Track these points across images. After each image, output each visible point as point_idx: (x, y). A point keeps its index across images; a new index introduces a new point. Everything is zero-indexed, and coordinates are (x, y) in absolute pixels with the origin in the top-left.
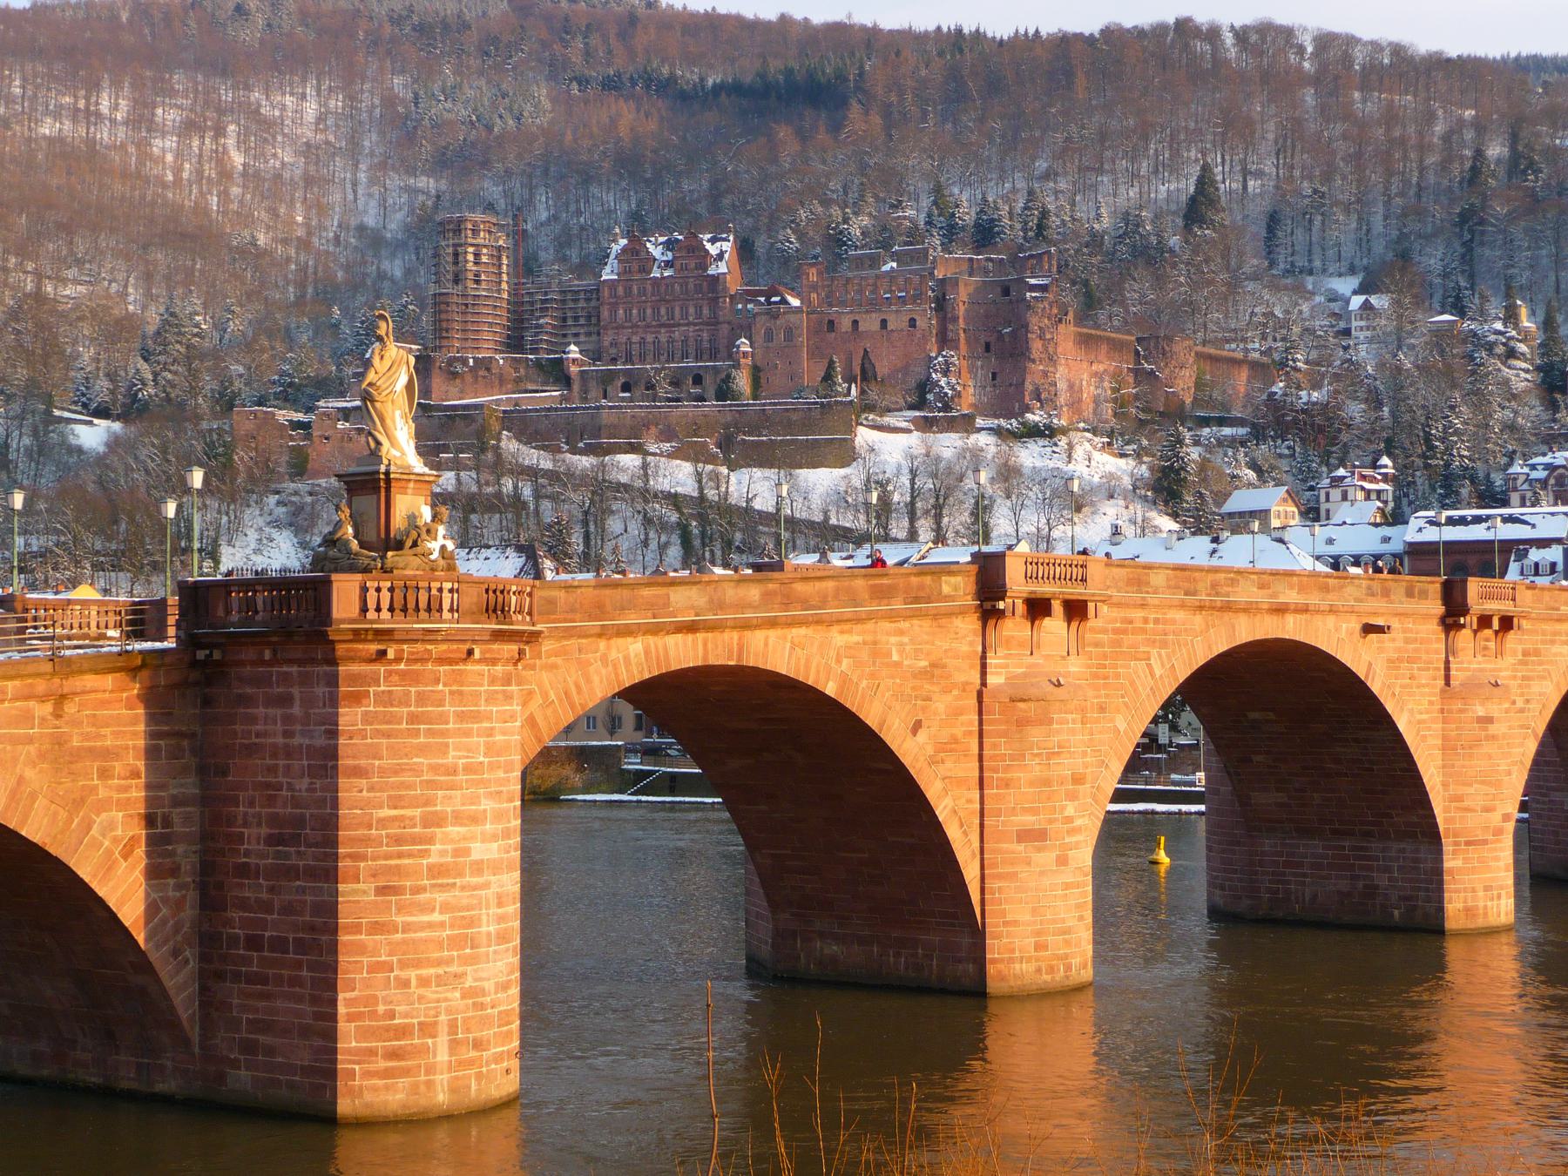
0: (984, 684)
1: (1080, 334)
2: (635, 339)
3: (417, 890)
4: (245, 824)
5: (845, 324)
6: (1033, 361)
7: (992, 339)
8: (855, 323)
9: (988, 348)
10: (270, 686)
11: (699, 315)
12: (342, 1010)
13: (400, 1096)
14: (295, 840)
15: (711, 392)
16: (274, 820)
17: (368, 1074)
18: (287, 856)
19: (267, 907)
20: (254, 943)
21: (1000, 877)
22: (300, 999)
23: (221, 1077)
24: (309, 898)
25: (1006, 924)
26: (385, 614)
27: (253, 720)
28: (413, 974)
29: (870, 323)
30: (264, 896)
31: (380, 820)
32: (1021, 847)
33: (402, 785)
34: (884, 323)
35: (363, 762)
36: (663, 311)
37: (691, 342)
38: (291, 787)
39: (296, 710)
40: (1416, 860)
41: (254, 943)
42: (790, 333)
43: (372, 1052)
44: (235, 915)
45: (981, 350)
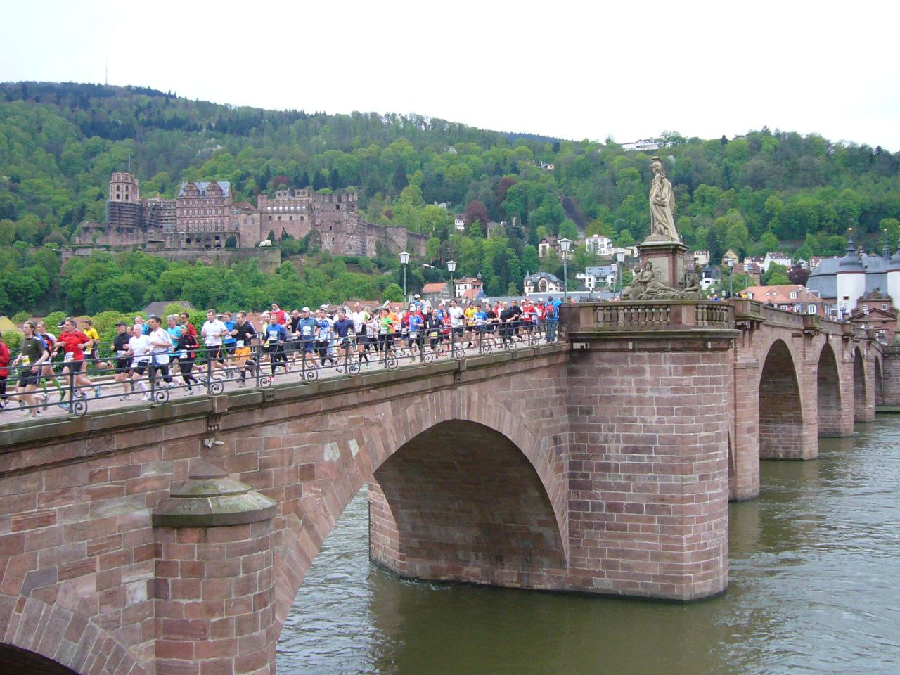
0: (736, 360)
3: (714, 476)
4: (606, 441)
5: (276, 217)
8: (280, 217)
10: (626, 362)
11: (216, 213)
12: (685, 544)
13: (709, 589)
14: (648, 450)
15: (223, 244)
16: (628, 439)
17: (698, 579)
18: (640, 459)
19: (626, 488)
20: (614, 507)
21: (743, 449)
22: (653, 538)
23: (589, 582)
24: (658, 483)
25: (744, 471)
26: (706, 324)
27: (613, 383)
28: (713, 522)
29: (286, 218)
30: (623, 481)
31: (701, 438)
32: (748, 435)
33: (710, 419)
34: (291, 217)
35: (693, 406)
38: (643, 420)
39: (647, 377)
40: (791, 432)
41: (614, 507)
42: (253, 221)
43: (698, 566)
44: (599, 492)
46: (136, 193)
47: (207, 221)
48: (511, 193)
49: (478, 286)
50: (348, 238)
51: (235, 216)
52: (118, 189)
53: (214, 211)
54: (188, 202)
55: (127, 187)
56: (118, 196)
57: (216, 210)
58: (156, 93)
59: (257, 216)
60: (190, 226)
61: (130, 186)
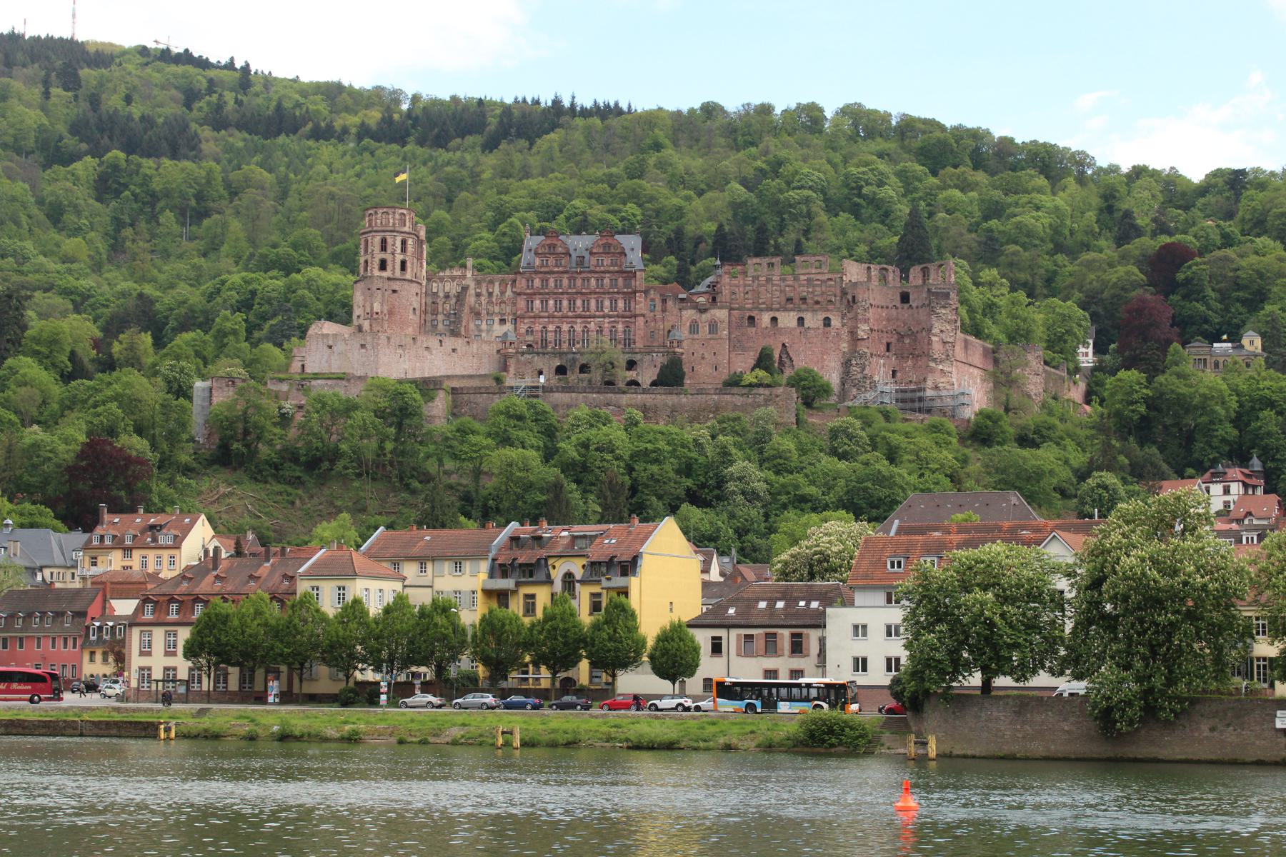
2: (551, 327)
5: (765, 319)
7: (893, 340)
8: (774, 320)
9: (888, 345)
11: (614, 307)
34: (801, 320)
36: (579, 303)
37: (606, 332)
42: (713, 327)
45: (883, 348)
46: (420, 259)
47: (592, 326)
48: (1188, 281)
49: (1254, 487)
50: (932, 371)
51: (659, 316)
52: (384, 247)
53: (607, 303)
54: (545, 282)
55: (404, 243)
56: (383, 265)
57: (614, 302)
58: (203, 63)
59: (721, 314)
60: (551, 337)
61: (410, 242)
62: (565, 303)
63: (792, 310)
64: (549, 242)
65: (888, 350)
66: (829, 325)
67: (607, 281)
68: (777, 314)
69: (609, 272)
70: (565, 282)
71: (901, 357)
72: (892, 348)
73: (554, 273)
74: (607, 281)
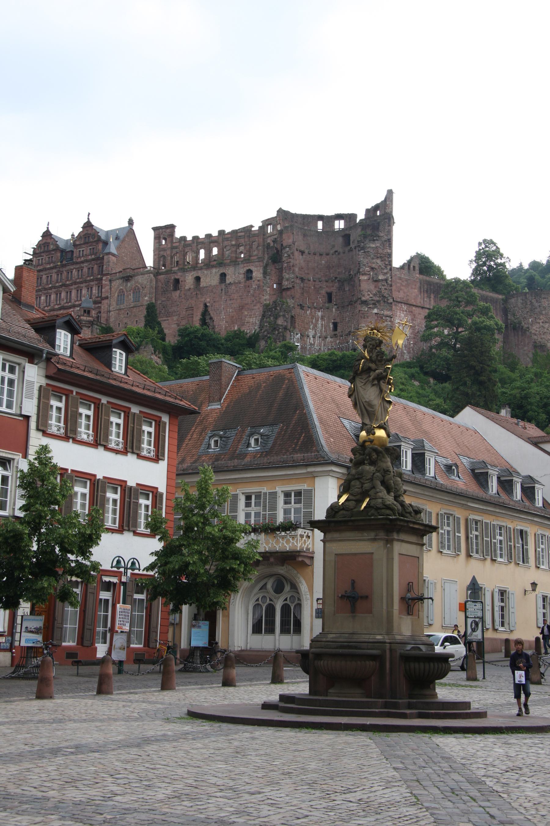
1: (429, 283)
5: (189, 280)
6: (365, 303)
8: (198, 279)
34: (223, 276)
45: (321, 300)
50: (364, 316)
62: (53, 297)
63: (213, 266)
64: (44, 241)
65: (330, 300)
66: (251, 278)
67: (85, 270)
68: (199, 274)
69: (86, 261)
70: (54, 276)
71: (341, 307)
72: (334, 299)
73: (45, 269)
74: (85, 270)
